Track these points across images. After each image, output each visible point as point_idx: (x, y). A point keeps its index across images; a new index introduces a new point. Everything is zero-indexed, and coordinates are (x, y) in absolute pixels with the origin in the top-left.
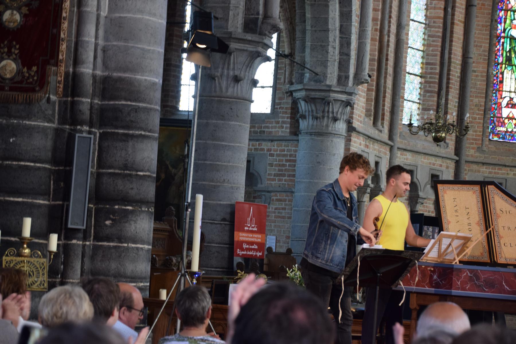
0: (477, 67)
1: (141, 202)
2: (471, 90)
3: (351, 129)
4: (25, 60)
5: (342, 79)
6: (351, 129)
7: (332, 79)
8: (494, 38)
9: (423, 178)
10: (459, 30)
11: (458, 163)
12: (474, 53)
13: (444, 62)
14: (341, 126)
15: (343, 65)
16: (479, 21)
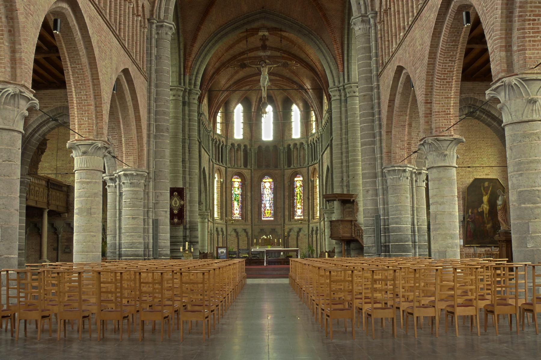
0: (229, 202)
1: (181, 242)
2: (228, 207)
3: (208, 221)
4: (179, 219)
5: (206, 210)
6: (208, 221)
7: (204, 210)
8: (232, 194)
9: (219, 229)
10: (224, 194)
11: (226, 225)
12: (228, 198)
13: (221, 202)
14: (207, 220)
15: (206, 207)
16: (228, 190)
